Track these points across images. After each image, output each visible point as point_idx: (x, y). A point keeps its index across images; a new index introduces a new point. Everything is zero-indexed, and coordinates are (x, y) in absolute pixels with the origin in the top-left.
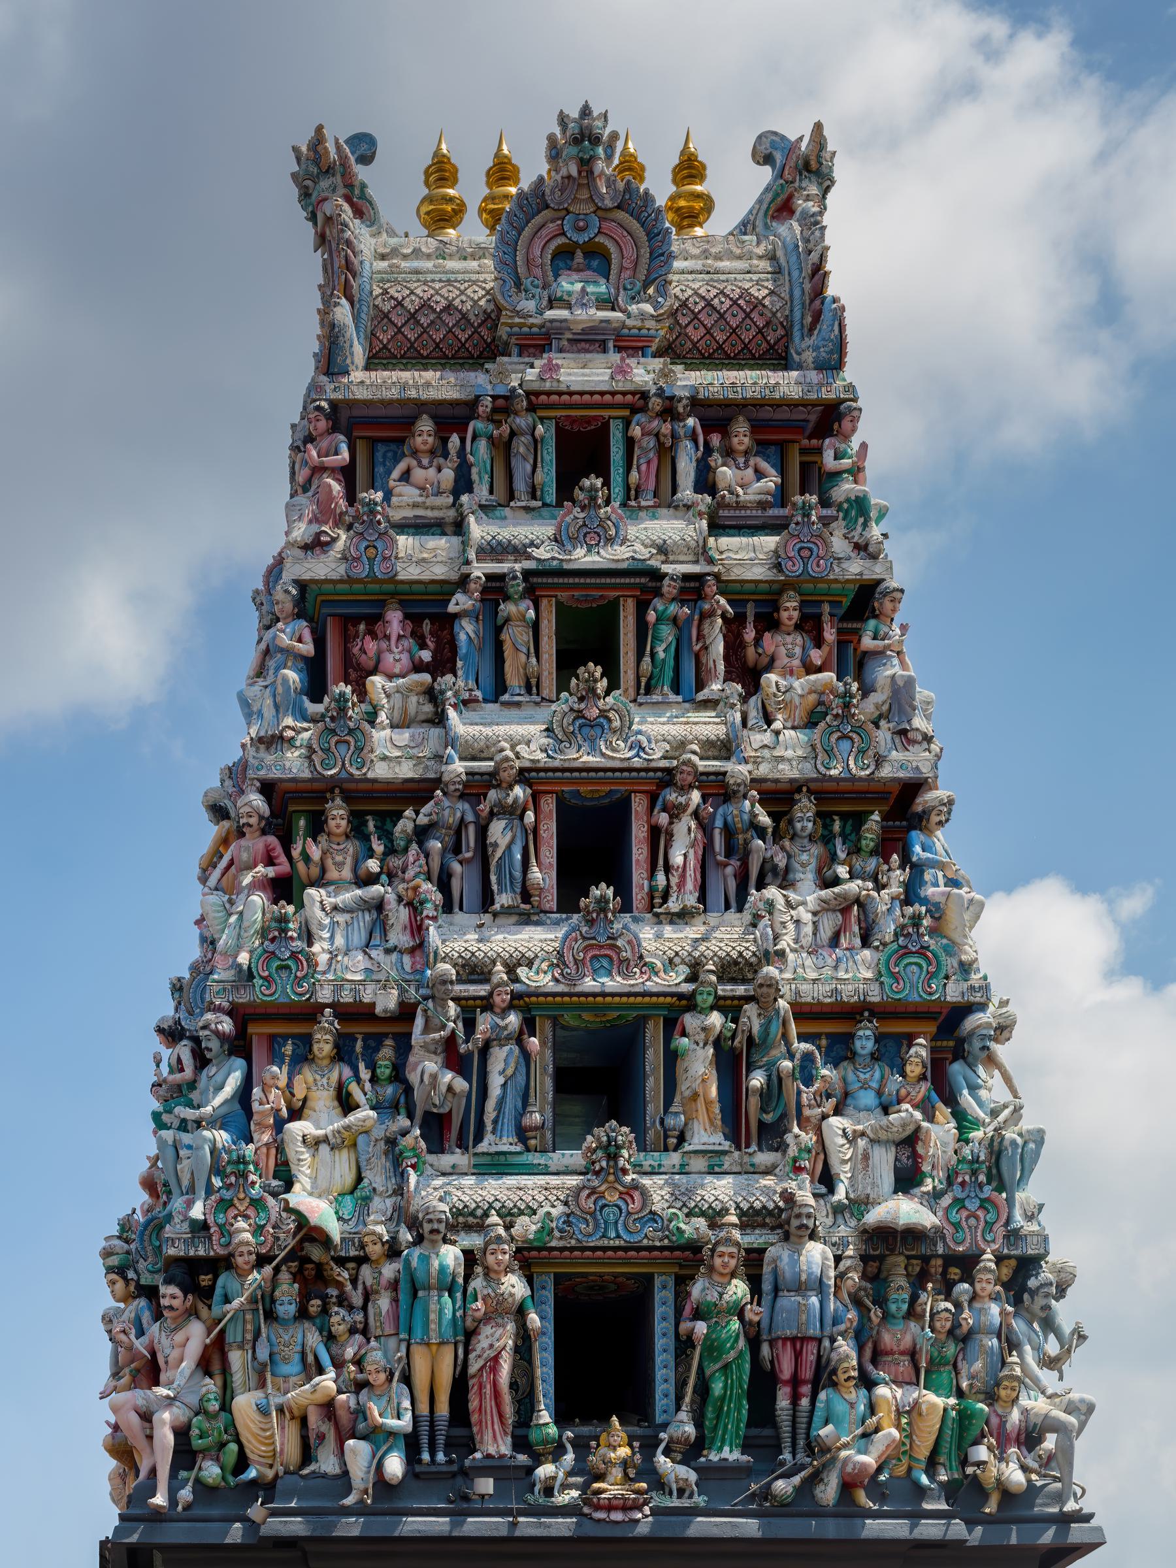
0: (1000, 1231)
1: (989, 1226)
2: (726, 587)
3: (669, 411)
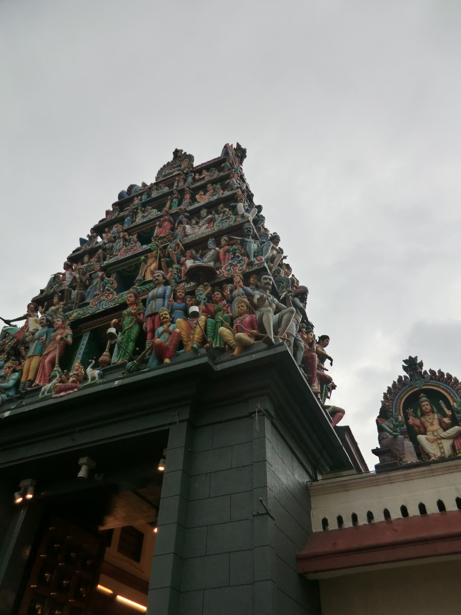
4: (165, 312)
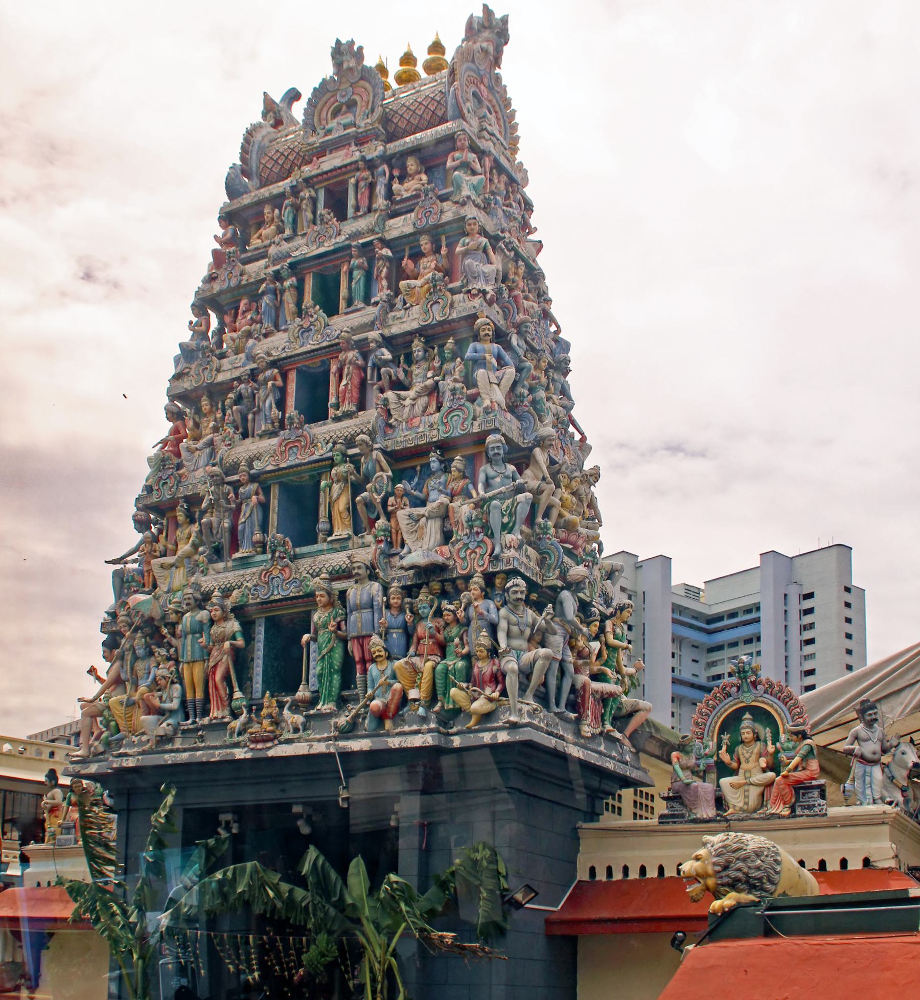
0: (487, 558)
1: (482, 556)
2: (386, 243)
3: (371, 165)
4: (378, 648)
